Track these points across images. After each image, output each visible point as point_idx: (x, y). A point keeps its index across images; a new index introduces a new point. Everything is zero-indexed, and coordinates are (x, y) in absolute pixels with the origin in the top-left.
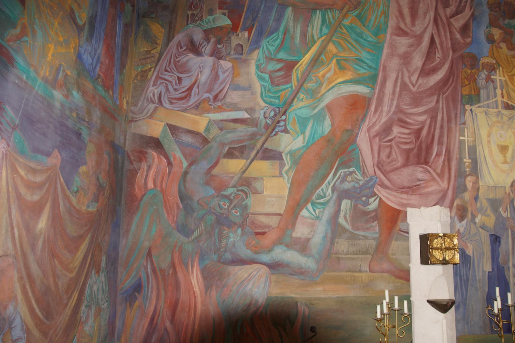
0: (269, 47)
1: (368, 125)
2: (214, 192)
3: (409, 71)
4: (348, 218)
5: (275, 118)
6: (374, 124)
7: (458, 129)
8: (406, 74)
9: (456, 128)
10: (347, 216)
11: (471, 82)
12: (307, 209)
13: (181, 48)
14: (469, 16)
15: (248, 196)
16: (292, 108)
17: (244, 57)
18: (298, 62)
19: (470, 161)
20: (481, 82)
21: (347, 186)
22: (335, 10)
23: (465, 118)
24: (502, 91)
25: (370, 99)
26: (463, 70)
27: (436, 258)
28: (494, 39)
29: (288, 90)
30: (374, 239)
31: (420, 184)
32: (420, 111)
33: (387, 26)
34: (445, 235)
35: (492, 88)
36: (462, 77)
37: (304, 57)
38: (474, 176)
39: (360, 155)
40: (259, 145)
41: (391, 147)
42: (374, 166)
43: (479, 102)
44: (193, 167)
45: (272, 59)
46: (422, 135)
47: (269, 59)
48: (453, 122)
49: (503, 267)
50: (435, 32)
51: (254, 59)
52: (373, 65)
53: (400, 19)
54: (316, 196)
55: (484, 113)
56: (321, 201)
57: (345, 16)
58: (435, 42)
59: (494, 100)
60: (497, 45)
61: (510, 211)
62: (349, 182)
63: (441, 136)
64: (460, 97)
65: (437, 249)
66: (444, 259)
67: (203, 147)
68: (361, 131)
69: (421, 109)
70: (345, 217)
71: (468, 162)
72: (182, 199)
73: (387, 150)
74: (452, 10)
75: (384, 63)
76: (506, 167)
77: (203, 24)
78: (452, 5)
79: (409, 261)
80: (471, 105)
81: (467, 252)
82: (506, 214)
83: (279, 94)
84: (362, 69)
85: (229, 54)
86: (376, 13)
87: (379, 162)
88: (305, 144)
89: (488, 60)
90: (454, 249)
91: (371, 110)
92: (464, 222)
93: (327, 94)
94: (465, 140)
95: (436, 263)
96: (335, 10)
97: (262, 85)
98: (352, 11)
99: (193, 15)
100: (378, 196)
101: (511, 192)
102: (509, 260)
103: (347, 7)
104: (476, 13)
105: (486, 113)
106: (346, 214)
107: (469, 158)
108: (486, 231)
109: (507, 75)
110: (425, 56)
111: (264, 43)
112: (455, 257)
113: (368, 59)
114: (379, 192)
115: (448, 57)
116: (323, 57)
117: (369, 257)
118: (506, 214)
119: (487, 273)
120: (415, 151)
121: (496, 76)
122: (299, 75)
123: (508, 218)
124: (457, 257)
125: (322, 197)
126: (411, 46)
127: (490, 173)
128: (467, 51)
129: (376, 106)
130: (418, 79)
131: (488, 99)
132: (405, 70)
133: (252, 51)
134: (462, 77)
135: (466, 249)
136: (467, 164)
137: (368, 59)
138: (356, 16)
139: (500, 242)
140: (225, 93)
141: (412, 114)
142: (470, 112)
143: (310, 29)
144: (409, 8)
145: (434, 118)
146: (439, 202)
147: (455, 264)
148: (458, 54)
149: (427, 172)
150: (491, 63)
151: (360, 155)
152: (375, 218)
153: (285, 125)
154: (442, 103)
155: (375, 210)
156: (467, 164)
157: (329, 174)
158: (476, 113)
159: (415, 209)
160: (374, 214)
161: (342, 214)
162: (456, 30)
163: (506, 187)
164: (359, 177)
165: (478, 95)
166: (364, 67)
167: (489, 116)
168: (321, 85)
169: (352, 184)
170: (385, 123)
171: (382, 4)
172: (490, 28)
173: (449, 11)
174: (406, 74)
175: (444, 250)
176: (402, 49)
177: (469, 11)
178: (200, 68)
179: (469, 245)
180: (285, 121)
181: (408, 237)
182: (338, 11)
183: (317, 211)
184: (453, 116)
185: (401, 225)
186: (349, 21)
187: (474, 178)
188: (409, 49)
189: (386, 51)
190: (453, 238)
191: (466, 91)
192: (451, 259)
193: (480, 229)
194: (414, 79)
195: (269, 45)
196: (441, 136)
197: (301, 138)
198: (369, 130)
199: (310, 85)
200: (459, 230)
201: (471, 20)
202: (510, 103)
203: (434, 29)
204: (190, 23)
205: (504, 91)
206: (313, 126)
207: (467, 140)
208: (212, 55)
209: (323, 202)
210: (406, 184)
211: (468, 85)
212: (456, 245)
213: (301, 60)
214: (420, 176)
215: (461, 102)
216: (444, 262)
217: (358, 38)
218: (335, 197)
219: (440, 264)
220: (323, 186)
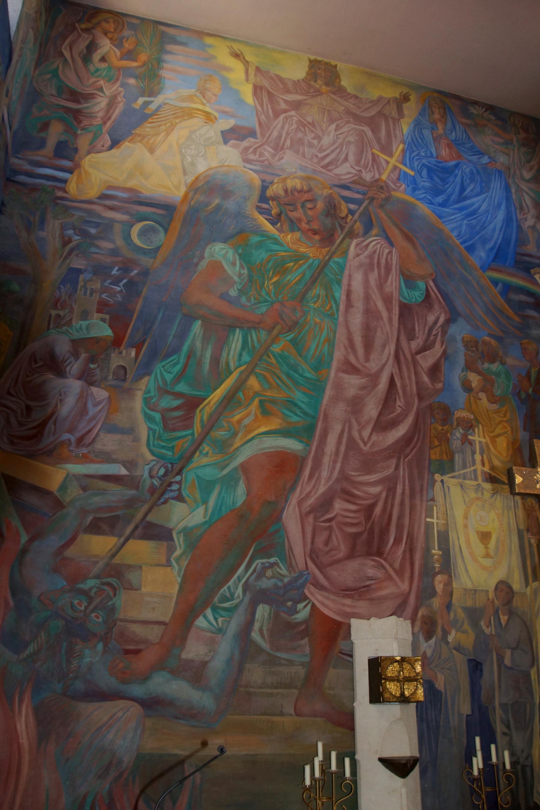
0: (165, 374)
1: (299, 497)
2: (65, 584)
3: (359, 424)
4: (265, 632)
5: (165, 478)
6: (308, 495)
7: (424, 507)
8: (355, 426)
9: (421, 506)
10: (265, 629)
11: (443, 442)
12: (205, 617)
13: (36, 362)
14: (439, 354)
15: (118, 592)
16: (191, 466)
17: (127, 385)
18: (204, 399)
19: (440, 553)
20: (456, 443)
21: (265, 583)
22: (261, 330)
23: (433, 491)
24: (482, 457)
25: (304, 459)
26: (432, 426)
27: (391, 694)
28: (471, 386)
29: (187, 439)
30: (302, 664)
31: (371, 584)
32: (373, 480)
33: (332, 359)
34: (403, 659)
35: (470, 452)
36: (430, 434)
37: (213, 393)
38: (445, 574)
39: (286, 540)
40: (139, 516)
41: (330, 528)
42: (305, 556)
43: (453, 471)
44: (36, 543)
45: (168, 392)
46: (375, 514)
47: (163, 391)
48: (418, 496)
49: (487, 708)
50: (396, 371)
51: (141, 389)
52: (310, 411)
53: (349, 350)
54: (219, 599)
55: (459, 487)
56: (226, 605)
57: (275, 340)
58: (396, 385)
59: (472, 468)
60: (475, 395)
61: (495, 625)
62: (269, 578)
63: (401, 517)
64: (427, 462)
65: (392, 679)
66: (402, 694)
67: (54, 514)
68: (289, 505)
69: (374, 477)
70: (261, 630)
71: (439, 555)
72: (14, 593)
73: (325, 534)
74: (418, 345)
75: (325, 409)
76: (487, 562)
77: (71, 332)
78: (418, 337)
79: (353, 699)
80: (442, 475)
81: (437, 686)
82: (490, 629)
83: (174, 443)
84: (294, 416)
85: (106, 378)
86: (317, 340)
87: (312, 551)
88: (207, 519)
89: (464, 414)
90: (416, 680)
91: (304, 475)
92: (432, 641)
93: (243, 448)
94: (434, 522)
95: (391, 700)
96: (261, 330)
97: (150, 429)
98: (285, 333)
99: (58, 316)
100: (310, 601)
101: (495, 599)
102: (494, 696)
103: (278, 327)
104: (449, 351)
105: (462, 486)
106: (262, 626)
107: (439, 549)
108: (463, 654)
109: (488, 436)
110: (382, 402)
111: (158, 368)
112: (417, 692)
113: (303, 402)
114: (312, 594)
115: (413, 406)
116: (241, 394)
117: (296, 692)
118: (490, 629)
119: (465, 716)
120: (364, 536)
121: (474, 436)
122: (205, 418)
123: (492, 635)
124: (420, 691)
125: (227, 600)
126: (363, 388)
127: (467, 571)
128: (437, 400)
129: (311, 469)
130: (371, 434)
131: (464, 467)
132: (354, 421)
133: (139, 377)
134: (430, 434)
135: (435, 681)
136: (436, 557)
137: (303, 402)
138: (291, 341)
139: (481, 670)
140: (94, 435)
141: (361, 483)
142: (441, 484)
143: (224, 354)
144: (362, 337)
145: (391, 491)
146: (398, 612)
147: (418, 702)
148: (425, 403)
149: (380, 568)
150: (468, 418)
151: (286, 540)
152: (304, 633)
153: (179, 490)
154: (404, 470)
155: (305, 622)
156: (436, 557)
157: (239, 566)
158: (449, 485)
159: (362, 620)
160: (303, 627)
161: (257, 626)
162: (424, 371)
163: (488, 591)
164: (284, 571)
165: (452, 460)
166: (298, 413)
167: (466, 490)
168: (235, 434)
169: (273, 581)
170: (323, 494)
171: (326, 327)
172: (467, 372)
173: (415, 345)
174: (355, 426)
175: (401, 681)
176: (351, 392)
177: (440, 347)
178: (61, 395)
179: (439, 676)
180: (179, 483)
181: (352, 663)
182: (266, 332)
183: (220, 620)
184: (418, 488)
185: (342, 645)
186: (280, 347)
187: (446, 577)
188: (360, 392)
189: (328, 392)
190: (414, 664)
191: (435, 454)
192: (412, 694)
193: (455, 652)
194: (366, 433)
195: (165, 371)
196: (401, 517)
197: (201, 510)
198: (300, 503)
199: (220, 434)
200: (425, 653)
201: (443, 360)
203: (394, 368)
204: (53, 328)
206: (220, 493)
207: (437, 523)
208: (80, 378)
209: (228, 606)
210: (350, 583)
211: (437, 446)
212: (419, 673)
213: (209, 396)
214: (371, 572)
215: (429, 469)
216: (403, 700)
217: (292, 372)
218: (247, 600)
219: (396, 702)
220: (231, 583)
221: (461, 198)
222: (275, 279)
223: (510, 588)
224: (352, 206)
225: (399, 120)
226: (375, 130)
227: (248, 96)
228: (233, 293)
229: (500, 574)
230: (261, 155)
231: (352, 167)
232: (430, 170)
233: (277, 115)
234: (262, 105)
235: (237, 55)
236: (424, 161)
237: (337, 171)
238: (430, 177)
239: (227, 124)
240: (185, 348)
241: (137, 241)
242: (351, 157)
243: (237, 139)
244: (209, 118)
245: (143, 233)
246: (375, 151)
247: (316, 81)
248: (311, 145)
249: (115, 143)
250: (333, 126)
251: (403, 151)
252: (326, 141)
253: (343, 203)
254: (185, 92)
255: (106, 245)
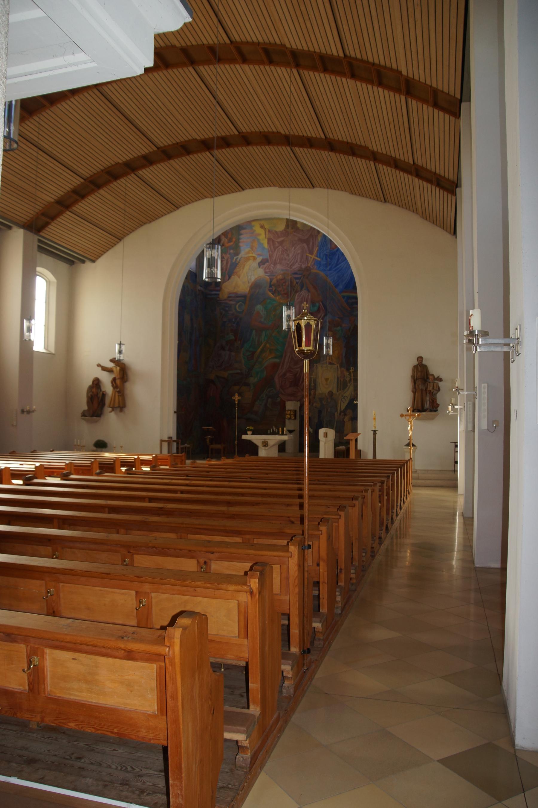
65: (288, 414)
105: (322, 366)
202: (332, 362)
205: (330, 358)
221: (337, 265)
222: (273, 313)
223: (332, 393)
224: (297, 281)
225: (318, 236)
226: (308, 245)
227: (266, 246)
228: (262, 320)
229: (330, 389)
230: (270, 269)
231: (299, 264)
232: (326, 255)
233: (275, 250)
234: (270, 248)
235: (262, 227)
236: (325, 252)
237: (294, 268)
238: (326, 259)
239: (259, 259)
240: (251, 339)
241: (238, 310)
242: (299, 260)
243: (263, 265)
244: (255, 259)
245: (239, 306)
246: (308, 254)
247: (288, 228)
248: (286, 259)
249: (230, 277)
250: (294, 248)
251: (318, 250)
252: (291, 255)
253: (295, 280)
254: (247, 250)
255: (231, 312)
